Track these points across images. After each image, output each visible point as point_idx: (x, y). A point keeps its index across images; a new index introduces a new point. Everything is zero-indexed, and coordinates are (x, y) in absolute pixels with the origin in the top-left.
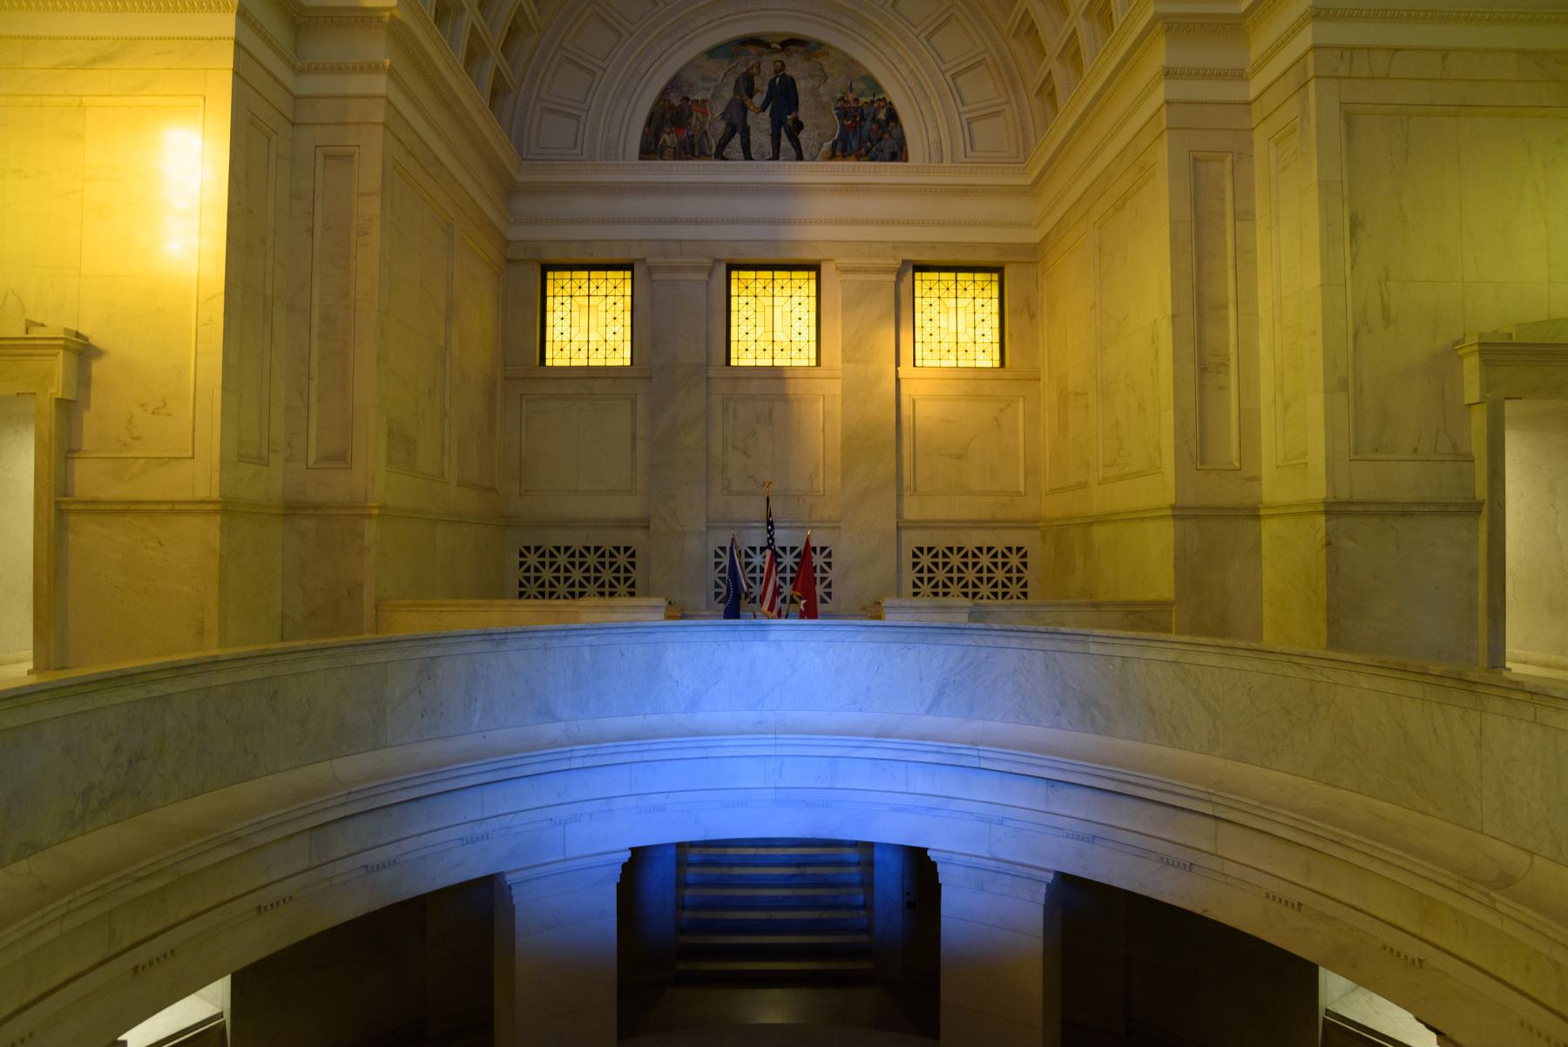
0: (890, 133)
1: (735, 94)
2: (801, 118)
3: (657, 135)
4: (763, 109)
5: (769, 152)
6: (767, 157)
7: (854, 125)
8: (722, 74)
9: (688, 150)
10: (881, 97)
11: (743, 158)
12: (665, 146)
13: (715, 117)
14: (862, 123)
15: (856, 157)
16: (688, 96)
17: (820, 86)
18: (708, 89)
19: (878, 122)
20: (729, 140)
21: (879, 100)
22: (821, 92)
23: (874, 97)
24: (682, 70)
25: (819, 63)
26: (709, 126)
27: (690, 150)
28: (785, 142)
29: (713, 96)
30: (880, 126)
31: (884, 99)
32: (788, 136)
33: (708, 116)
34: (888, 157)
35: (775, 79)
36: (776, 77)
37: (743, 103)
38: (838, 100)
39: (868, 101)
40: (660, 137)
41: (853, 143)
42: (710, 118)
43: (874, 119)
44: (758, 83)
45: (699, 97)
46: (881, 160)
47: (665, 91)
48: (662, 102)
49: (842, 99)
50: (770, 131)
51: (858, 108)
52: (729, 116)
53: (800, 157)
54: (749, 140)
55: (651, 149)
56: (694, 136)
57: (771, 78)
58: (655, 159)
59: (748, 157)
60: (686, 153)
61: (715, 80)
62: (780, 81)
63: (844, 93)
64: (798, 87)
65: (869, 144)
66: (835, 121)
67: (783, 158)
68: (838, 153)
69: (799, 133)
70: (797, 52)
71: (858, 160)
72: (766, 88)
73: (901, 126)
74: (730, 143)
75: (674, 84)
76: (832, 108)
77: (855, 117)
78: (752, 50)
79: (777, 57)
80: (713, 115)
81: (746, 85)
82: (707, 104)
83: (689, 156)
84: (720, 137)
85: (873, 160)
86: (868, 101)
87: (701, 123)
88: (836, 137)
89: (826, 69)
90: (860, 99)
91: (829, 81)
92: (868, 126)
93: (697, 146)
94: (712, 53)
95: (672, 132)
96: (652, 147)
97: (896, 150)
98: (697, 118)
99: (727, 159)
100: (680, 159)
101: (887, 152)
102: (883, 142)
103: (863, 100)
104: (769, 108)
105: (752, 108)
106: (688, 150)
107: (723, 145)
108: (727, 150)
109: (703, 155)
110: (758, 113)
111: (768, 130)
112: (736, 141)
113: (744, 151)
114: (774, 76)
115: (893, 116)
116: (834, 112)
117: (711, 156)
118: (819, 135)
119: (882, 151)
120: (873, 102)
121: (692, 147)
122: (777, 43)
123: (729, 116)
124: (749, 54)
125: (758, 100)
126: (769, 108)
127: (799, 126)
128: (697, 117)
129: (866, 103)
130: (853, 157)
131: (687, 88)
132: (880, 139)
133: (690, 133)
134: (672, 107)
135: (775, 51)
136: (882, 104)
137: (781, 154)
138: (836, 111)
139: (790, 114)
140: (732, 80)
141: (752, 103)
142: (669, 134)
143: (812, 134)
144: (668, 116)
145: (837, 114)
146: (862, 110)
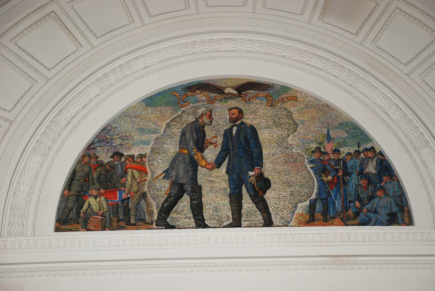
2: (266, 175)
3: (80, 198)
4: (218, 164)
5: (228, 217)
6: (225, 224)
7: (336, 181)
8: (164, 126)
9: (121, 217)
10: (369, 146)
12: (90, 212)
13: (156, 175)
15: (342, 220)
16: (121, 151)
17: (289, 136)
18: (146, 143)
19: (368, 177)
20: (175, 204)
21: (366, 150)
22: (291, 143)
23: (359, 147)
24: (114, 121)
28: (248, 204)
29: (153, 150)
30: (370, 183)
31: (373, 148)
35: (231, 129)
36: (233, 126)
37: (192, 158)
38: (312, 152)
39: (352, 152)
40: (85, 201)
41: (336, 202)
42: (149, 177)
43: (361, 173)
44: (209, 133)
45: (135, 152)
47: (90, 147)
48: (86, 159)
49: (318, 149)
50: (228, 191)
51: (340, 160)
52: (174, 174)
53: (268, 223)
54: (201, 202)
57: (227, 128)
59: (201, 223)
61: (155, 131)
62: (237, 131)
63: (320, 143)
65: (357, 203)
67: (246, 223)
68: (318, 215)
70: (256, 97)
71: (346, 225)
72: (220, 140)
73: (398, 180)
74: (175, 209)
76: (306, 161)
77: (337, 171)
79: (233, 103)
80: (153, 173)
83: (122, 224)
84: (163, 200)
86: (352, 152)
87: (138, 183)
88: (313, 196)
89: (295, 116)
90: (341, 149)
91: (301, 129)
92: (354, 180)
93: (132, 213)
95: (100, 195)
96: (73, 215)
97: (394, 211)
98: (133, 176)
99: (173, 227)
100: (112, 229)
101: (383, 215)
102: (376, 200)
104: (226, 163)
106: (121, 217)
108: (173, 215)
110: (211, 169)
111: (225, 189)
112: (185, 203)
113: (194, 216)
114: (232, 124)
116: (309, 166)
117: (152, 224)
119: (375, 212)
120: (358, 152)
121: (127, 212)
122: (232, 87)
123: (174, 174)
125: (211, 154)
126: (226, 163)
127: (265, 184)
128: (133, 176)
129: (349, 154)
131: (119, 141)
132: (371, 198)
133: (124, 196)
134: (101, 164)
136: (370, 154)
138: (311, 165)
140: (177, 131)
142: (96, 198)
143: (284, 194)
144: (95, 175)
145: (312, 168)
146: (345, 163)
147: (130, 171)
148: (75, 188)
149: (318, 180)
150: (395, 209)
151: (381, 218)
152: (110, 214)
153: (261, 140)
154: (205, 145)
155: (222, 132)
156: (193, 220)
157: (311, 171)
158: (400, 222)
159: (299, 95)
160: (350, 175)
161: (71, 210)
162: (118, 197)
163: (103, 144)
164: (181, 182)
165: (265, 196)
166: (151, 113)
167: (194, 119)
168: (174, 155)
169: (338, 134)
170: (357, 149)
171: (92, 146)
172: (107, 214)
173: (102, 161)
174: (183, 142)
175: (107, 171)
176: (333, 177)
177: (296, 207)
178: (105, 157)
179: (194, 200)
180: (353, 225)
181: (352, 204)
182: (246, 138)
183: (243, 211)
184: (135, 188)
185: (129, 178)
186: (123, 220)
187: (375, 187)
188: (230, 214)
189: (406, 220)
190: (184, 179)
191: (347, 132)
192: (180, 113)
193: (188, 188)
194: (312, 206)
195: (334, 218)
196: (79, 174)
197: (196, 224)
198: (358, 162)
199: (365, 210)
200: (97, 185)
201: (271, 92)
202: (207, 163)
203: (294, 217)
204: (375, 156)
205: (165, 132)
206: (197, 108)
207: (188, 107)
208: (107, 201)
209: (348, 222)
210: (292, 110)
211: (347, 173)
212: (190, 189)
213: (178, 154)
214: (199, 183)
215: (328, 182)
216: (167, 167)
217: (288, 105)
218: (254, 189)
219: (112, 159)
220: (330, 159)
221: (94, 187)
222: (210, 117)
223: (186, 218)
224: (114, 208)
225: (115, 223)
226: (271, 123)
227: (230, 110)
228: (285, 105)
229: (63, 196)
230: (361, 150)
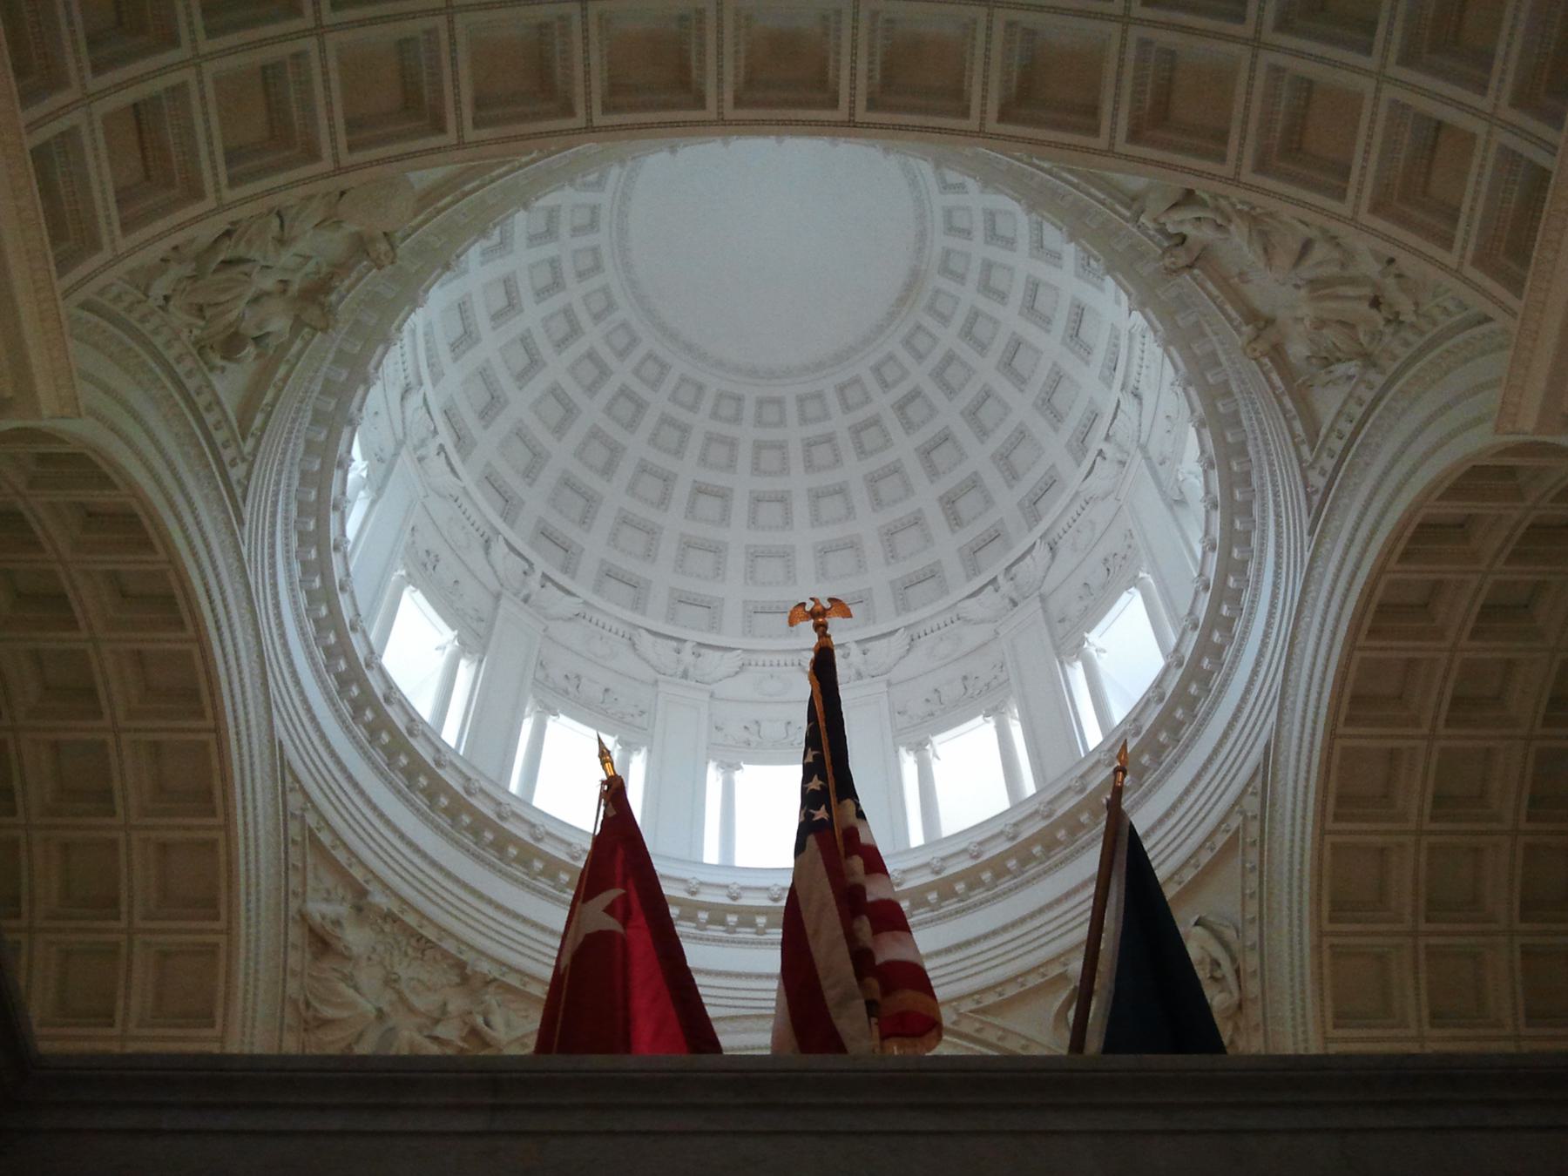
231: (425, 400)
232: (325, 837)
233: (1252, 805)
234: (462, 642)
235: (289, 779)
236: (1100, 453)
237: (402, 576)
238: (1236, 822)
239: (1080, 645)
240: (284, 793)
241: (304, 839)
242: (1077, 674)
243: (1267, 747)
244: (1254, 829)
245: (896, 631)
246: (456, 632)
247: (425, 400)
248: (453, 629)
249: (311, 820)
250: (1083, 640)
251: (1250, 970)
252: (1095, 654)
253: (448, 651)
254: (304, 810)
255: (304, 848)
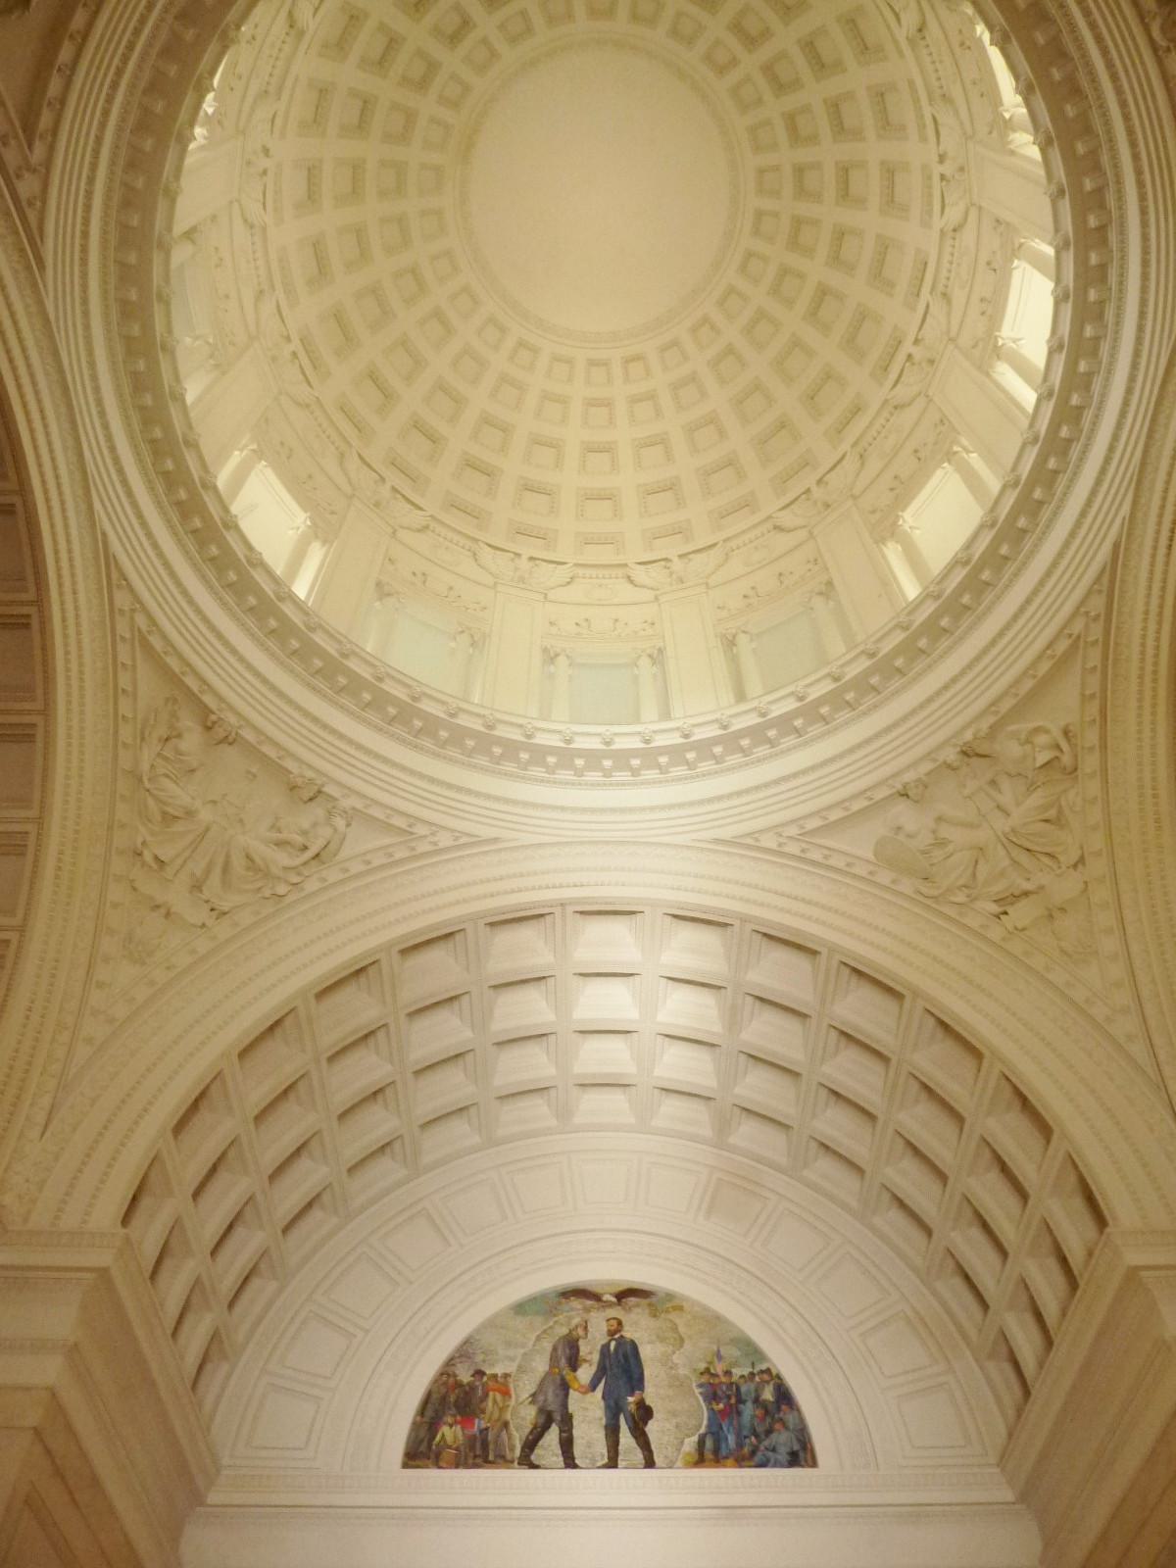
0: (786, 1428)
1: (551, 1367)
2: (648, 1402)
3: (433, 1426)
4: (593, 1387)
5: (603, 1456)
6: (599, 1464)
8: (534, 1339)
9: (478, 1452)
10: (764, 1367)
11: (562, 1464)
12: (445, 1446)
13: (521, 1400)
14: (741, 1406)
15: (736, 1460)
16: (483, 1369)
17: (674, 1353)
18: (512, 1359)
21: (762, 1372)
22: (676, 1361)
24: (478, 1331)
25: (671, 1321)
26: (512, 1415)
27: (481, 1453)
28: (626, 1438)
29: (520, 1367)
30: (767, 1412)
31: (768, 1371)
32: (630, 1428)
33: (510, 1397)
34: (783, 1456)
36: (610, 1341)
38: (702, 1374)
41: (730, 1438)
42: (513, 1402)
43: (757, 1401)
44: (584, 1349)
45: (499, 1370)
46: (775, 1465)
47: (450, 1362)
49: (707, 1371)
50: (604, 1422)
51: (732, 1384)
52: (541, 1398)
53: (650, 1463)
54: (571, 1434)
55: (421, 1452)
56: (487, 1429)
58: (426, 1467)
59: (570, 1462)
60: (475, 1457)
61: (523, 1346)
63: (710, 1363)
64: (642, 1355)
65: (753, 1438)
66: (699, 1404)
67: (624, 1463)
68: (708, 1455)
69: (646, 1424)
70: (638, 1306)
71: (741, 1467)
72: (596, 1357)
73: (799, 1410)
74: (540, 1443)
75: (463, 1352)
76: (694, 1384)
78: (576, 1304)
80: (517, 1396)
81: (570, 1352)
82: (510, 1380)
83: (479, 1461)
85: (762, 1465)
88: (703, 1430)
89: (682, 1329)
90: (734, 1371)
91: (687, 1345)
92: (748, 1410)
93: (491, 1447)
94: (520, 1308)
95: (456, 1422)
96: (423, 1448)
98: (495, 1401)
99: (536, 1467)
100: (467, 1466)
101: (783, 1455)
103: (737, 1372)
104: (601, 1385)
105: (576, 1386)
106: (478, 1452)
107: (531, 1445)
108: (538, 1451)
109: (501, 1460)
110: (585, 1393)
111: (601, 1419)
112: (553, 1436)
113: (563, 1453)
114: (610, 1338)
115: (784, 1396)
116: (697, 1391)
117: (512, 1462)
118: (677, 1426)
119: (774, 1450)
120: (752, 1375)
123: (541, 1398)
124: (572, 1309)
125: (585, 1374)
126: (601, 1385)
127: (645, 1413)
128: (495, 1401)
129: (742, 1376)
130: (730, 1461)
132: (769, 1432)
133: (483, 1426)
134: (459, 1385)
135: (610, 1305)
136: (766, 1377)
137: (620, 1458)
138: (700, 1390)
139: (632, 1395)
140: (547, 1345)
141: (575, 1378)
142: (451, 1426)
143: (668, 1425)
144: (452, 1398)
145: (701, 1393)
146: (738, 1389)
147: (491, 1393)
148: (429, 1413)
149: (708, 1409)
150: (796, 1447)
151: (779, 1457)
152: (465, 1448)
153: (642, 1355)
154: (579, 1363)
155: (599, 1348)
156: (561, 1459)
157: (701, 1399)
158: (803, 1463)
159: (684, 1304)
160: (743, 1402)
161: (422, 1441)
162: (479, 1424)
163: (464, 1359)
164: (549, 1408)
165: (647, 1429)
166: (520, 1322)
167: (568, 1331)
168: (543, 1375)
169: (731, 1352)
170: (751, 1370)
171: (453, 1362)
172: (462, 1449)
173: (461, 1381)
174: (554, 1360)
175: (466, 1393)
176: (725, 1407)
177: (682, 1443)
178: (465, 1376)
179: (564, 1432)
180: (750, 1467)
181: (747, 1441)
182: (626, 1357)
183: (620, 1448)
184: (496, 1415)
185: (490, 1403)
186: (479, 1456)
187: (773, 1418)
188: (605, 1451)
189: (810, 1461)
190: (553, 1405)
191: (739, 1349)
192: (551, 1324)
193: (557, 1417)
194: (701, 1443)
195: (726, 1458)
196: (435, 1396)
197: (565, 1463)
198: (752, 1386)
199: (762, 1448)
200: (453, 1411)
201: (653, 1300)
202: (582, 1386)
203: (681, 1456)
204: (772, 1379)
205: (534, 1345)
206: (570, 1318)
207: (561, 1317)
208: (463, 1430)
209: (743, 1464)
210: (678, 1321)
211: (740, 1401)
212: (559, 1418)
213: (548, 1374)
214: (570, 1411)
215: (720, 1412)
216: (534, 1390)
217: (673, 1316)
218: (634, 1418)
219: (472, 1379)
220: (721, 1383)
221: (451, 1412)
222: (586, 1328)
223: (553, 1455)
224: (471, 1441)
225: (471, 1461)
226: (654, 1338)
227: (608, 1320)
228: (670, 1316)
229: (414, 1423)
230: (755, 1371)
231: (278, 306)
232: (156, 642)
233: (1097, 604)
234: (314, 524)
235: (115, 575)
236: (910, 356)
237: (253, 450)
238: (1078, 627)
239: (895, 524)
240: (110, 592)
241: (133, 639)
242: (893, 553)
243: (1116, 546)
244: (1096, 632)
245: (715, 545)
246: (308, 514)
247: (278, 306)
248: (306, 512)
249: (141, 621)
250: (898, 517)
251: (1088, 771)
252: (909, 530)
253: (301, 530)
254: (133, 611)
255: (133, 645)
